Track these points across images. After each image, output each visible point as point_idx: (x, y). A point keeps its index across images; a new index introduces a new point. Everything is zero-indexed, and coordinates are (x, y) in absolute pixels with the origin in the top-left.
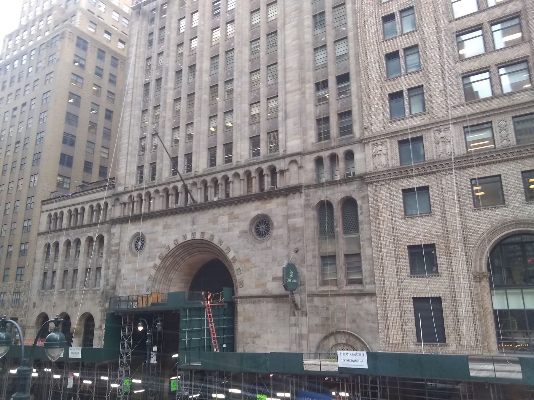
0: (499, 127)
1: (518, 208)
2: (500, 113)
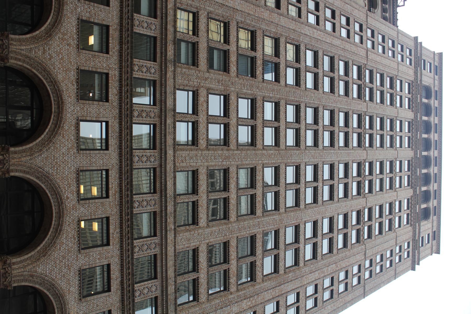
0: (151, 23)
1: (76, 9)
2: (162, 28)
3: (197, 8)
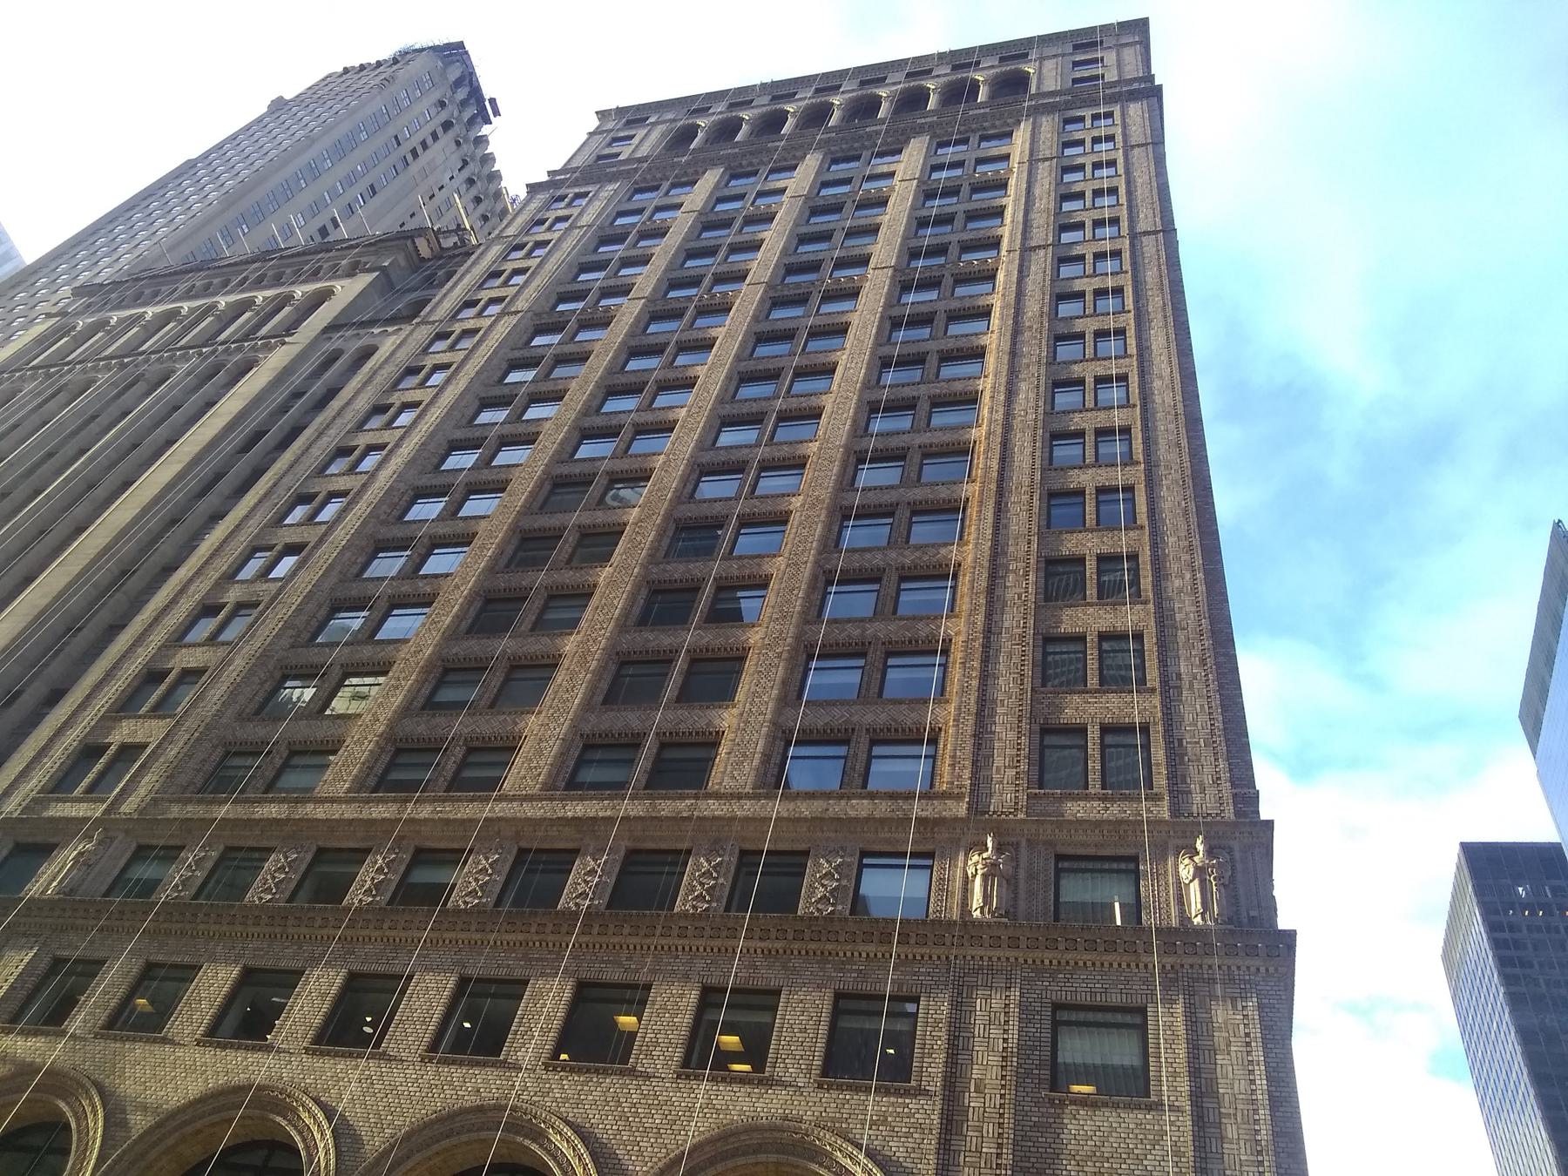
3: (215, 747)
